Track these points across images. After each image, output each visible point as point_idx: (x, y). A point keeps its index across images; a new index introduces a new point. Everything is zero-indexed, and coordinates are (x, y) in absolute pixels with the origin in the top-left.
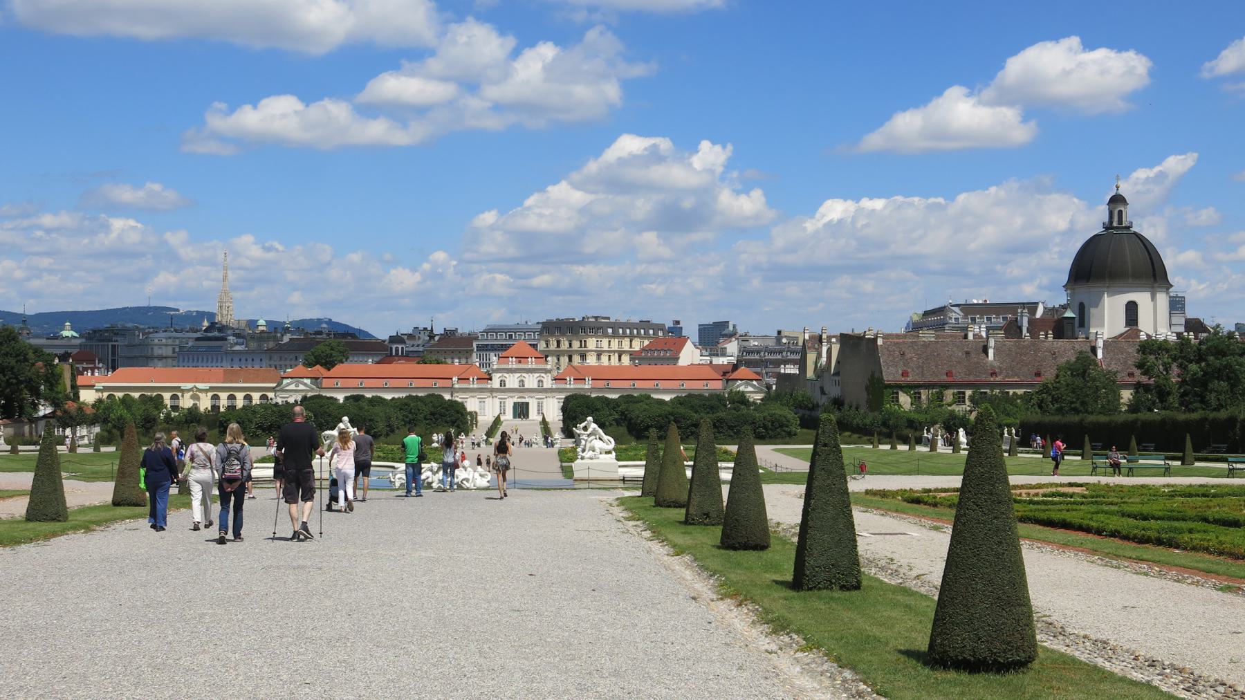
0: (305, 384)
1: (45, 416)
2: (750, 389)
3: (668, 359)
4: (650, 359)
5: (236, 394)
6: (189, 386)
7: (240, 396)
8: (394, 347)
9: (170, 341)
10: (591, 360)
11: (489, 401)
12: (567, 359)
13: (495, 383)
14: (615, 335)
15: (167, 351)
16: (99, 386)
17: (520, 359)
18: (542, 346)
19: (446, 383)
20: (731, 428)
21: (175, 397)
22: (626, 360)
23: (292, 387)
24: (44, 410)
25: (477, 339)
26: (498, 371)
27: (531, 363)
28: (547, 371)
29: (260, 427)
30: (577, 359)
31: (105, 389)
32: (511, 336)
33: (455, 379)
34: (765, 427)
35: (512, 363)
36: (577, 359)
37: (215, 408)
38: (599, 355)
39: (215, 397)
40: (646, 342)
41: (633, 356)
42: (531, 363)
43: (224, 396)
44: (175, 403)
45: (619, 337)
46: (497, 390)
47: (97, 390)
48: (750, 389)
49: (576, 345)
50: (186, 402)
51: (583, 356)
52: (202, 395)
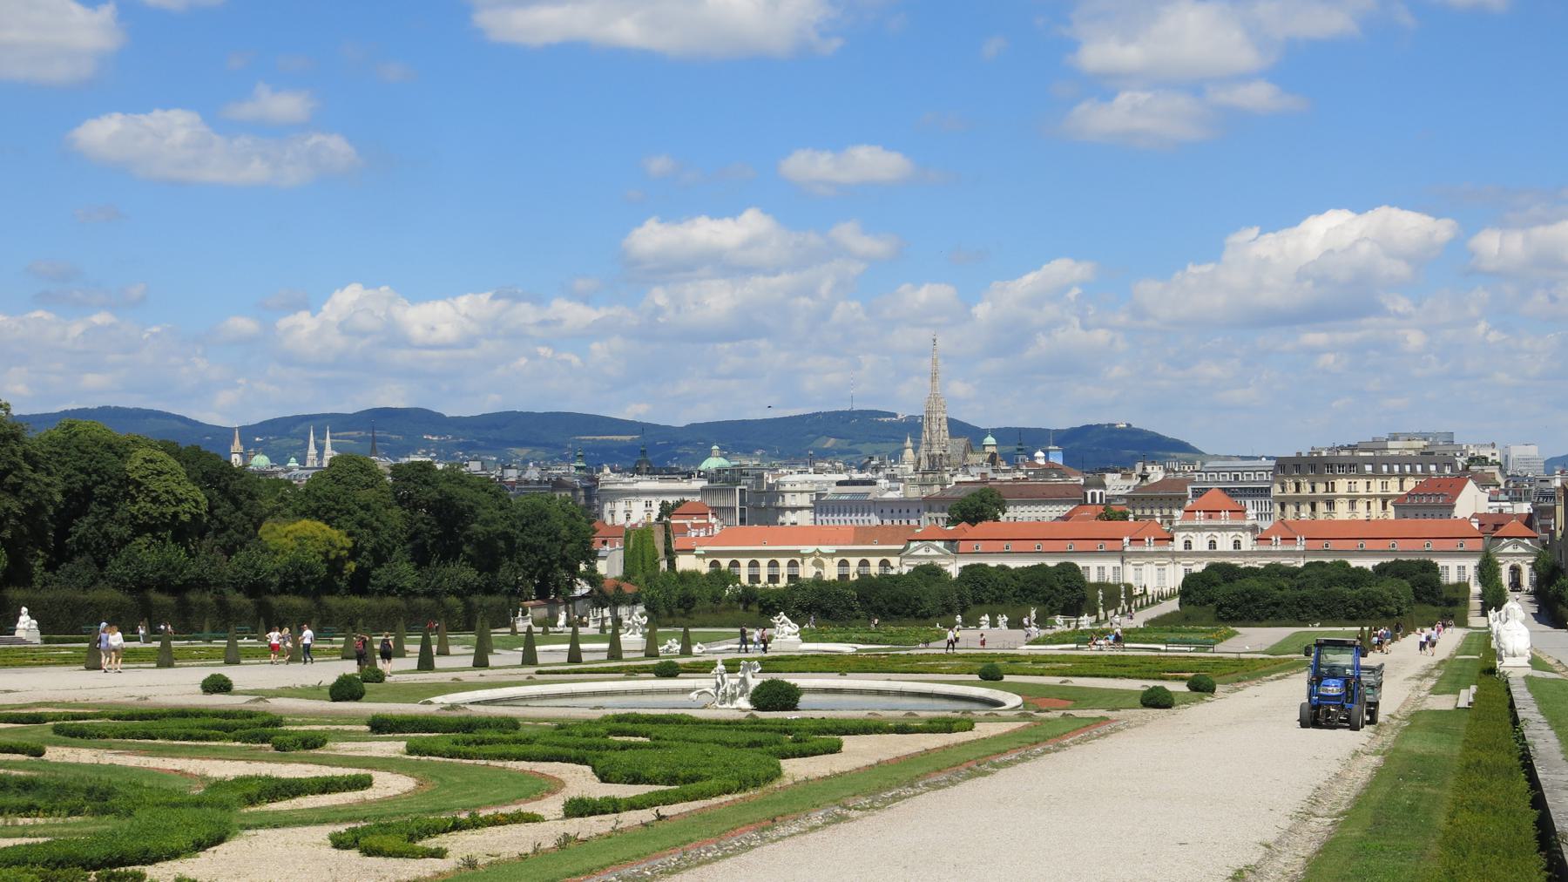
0: (937, 549)
1: (583, 597)
2: (1521, 550)
3: (1441, 507)
4: (1417, 507)
5: (870, 559)
6: (810, 549)
7: (874, 562)
8: (1089, 493)
9: (806, 487)
10: (1342, 512)
11: (1170, 568)
12: (1309, 508)
13: (1178, 545)
14: (1376, 474)
15: (804, 500)
16: (700, 550)
17: (1211, 512)
18: (1276, 490)
19: (1115, 545)
20: (1317, 607)
21: (793, 564)
22: (1391, 512)
23: (921, 552)
24: (583, 588)
25: (1192, 481)
26: (1181, 529)
27: (1225, 519)
28: (1244, 529)
29: (800, 607)
30: (1322, 507)
31: (708, 554)
32: (1236, 477)
33: (1126, 540)
34: (1356, 607)
35: (1200, 519)
36: (1322, 507)
37: (843, 577)
38: (1353, 502)
39: (844, 564)
40: (1410, 484)
41: (1404, 505)
42: (1225, 519)
43: (854, 562)
44: (793, 571)
45: (1382, 476)
46: (1179, 554)
47: (698, 556)
48: (1521, 550)
49: (1321, 489)
50: (807, 571)
51: (1330, 503)
52: (826, 561)
